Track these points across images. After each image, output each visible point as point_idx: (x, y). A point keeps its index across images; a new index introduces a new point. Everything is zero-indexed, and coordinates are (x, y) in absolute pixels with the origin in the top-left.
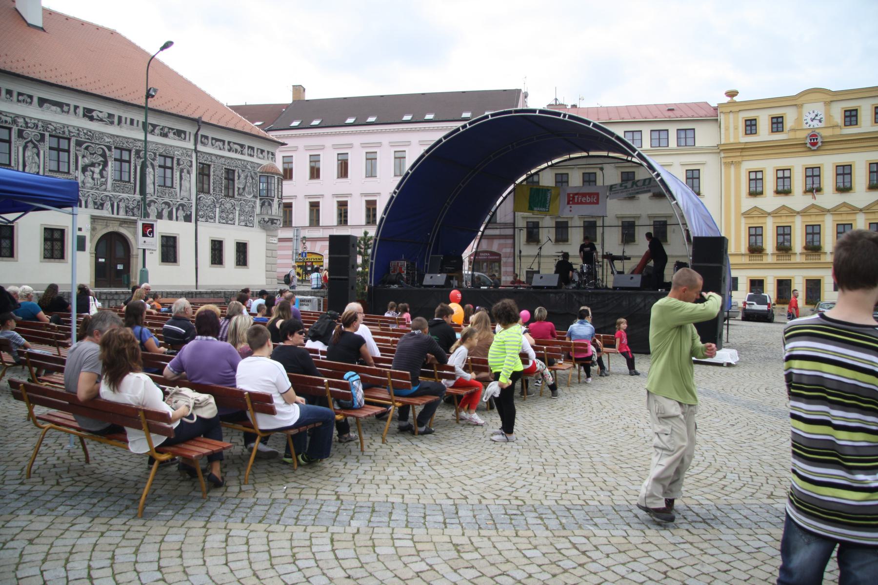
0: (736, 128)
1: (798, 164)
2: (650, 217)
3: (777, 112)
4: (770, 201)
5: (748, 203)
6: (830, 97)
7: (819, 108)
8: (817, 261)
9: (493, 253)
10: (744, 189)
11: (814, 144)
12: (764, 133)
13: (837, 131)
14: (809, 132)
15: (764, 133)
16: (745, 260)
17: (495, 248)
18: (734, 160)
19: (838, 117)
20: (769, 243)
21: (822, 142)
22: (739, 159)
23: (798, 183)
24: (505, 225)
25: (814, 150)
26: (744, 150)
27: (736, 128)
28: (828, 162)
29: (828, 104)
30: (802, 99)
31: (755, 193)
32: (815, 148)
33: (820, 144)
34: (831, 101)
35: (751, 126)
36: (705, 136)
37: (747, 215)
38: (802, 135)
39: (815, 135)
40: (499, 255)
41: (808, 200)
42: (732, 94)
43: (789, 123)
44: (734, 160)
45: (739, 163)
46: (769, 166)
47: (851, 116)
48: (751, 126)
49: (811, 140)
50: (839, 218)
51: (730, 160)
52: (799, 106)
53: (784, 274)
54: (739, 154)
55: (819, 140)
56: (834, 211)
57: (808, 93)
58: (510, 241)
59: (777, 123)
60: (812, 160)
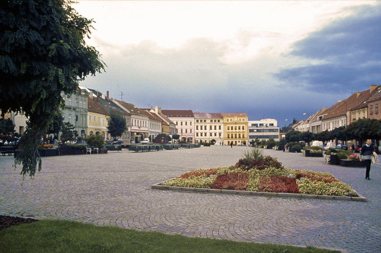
1: (234, 126)
4: (230, 131)
5: (228, 131)
10: (227, 129)
16: (227, 138)
17: (185, 137)
19: (239, 120)
20: (230, 137)
23: (234, 128)
24: (193, 133)
26: (227, 123)
28: (237, 126)
29: (237, 118)
35: (228, 120)
37: (227, 132)
41: (235, 131)
43: (233, 120)
45: (226, 125)
46: (230, 126)
52: (234, 118)
56: (238, 132)
60: (236, 125)
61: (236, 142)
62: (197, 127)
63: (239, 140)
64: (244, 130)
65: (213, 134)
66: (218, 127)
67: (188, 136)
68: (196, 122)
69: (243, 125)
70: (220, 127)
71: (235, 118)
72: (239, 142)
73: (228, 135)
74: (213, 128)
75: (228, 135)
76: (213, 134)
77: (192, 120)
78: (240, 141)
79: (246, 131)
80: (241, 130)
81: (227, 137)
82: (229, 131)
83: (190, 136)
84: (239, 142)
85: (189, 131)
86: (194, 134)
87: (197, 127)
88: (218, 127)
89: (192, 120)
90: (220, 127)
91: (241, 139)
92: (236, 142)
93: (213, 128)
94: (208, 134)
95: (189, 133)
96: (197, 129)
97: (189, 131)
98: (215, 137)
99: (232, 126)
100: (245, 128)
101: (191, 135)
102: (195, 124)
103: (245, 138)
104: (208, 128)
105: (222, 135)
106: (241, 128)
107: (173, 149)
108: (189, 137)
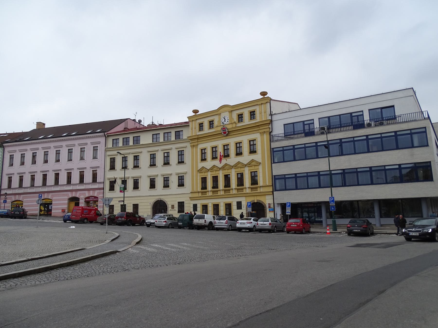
0: (195, 128)
1: (220, 143)
2: (162, 175)
3: (211, 119)
4: (209, 163)
6: (231, 109)
7: (226, 115)
8: (228, 194)
9: (96, 197)
11: (225, 133)
12: (206, 130)
13: (234, 125)
14: (222, 127)
15: (206, 130)
16: (200, 195)
18: (195, 144)
19: (235, 119)
21: (228, 131)
22: (196, 144)
24: (100, 183)
25: (225, 136)
27: (195, 128)
28: (232, 141)
30: (221, 110)
31: (204, 159)
32: (225, 135)
33: (227, 133)
34: (232, 111)
36: (186, 134)
37: (200, 171)
38: (219, 129)
39: (224, 128)
40: (98, 198)
42: (195, 111)
43: (216, 123)
44: (195, 144)
46: (208, 145)
47: (240, 117)
48: (201, 126)
49: (223, 131)
50: (237, 170)
51: (192, 144)
53: (216, 201)
54: (197, 141)
55: (227, 131)
57: (222, 108)
58: (102, 191)
59: (211, 123)
60: (225, 141)
61: (228, 206)
62: (113, 161)
63: (239, 199)
64: (257, 157)
65: (159, 183)
66: (174, 158)
67: (86, 192)
68: (110, 145)
69: (252, 137)
70: (181, 154)
71: (223, 115)
72: (239, 205)
73: (204, 180)
74: (160, 160)
75: (204, 180)
76: (159, 183)
77: (99, 143)
78: (244, 202)
79: (263, 157)
80: (246, 158)
81: (199, 189)
82: (204, 164)
83: (91, 193)
84: (239, 205)
85: (88, 178)
86: (101, 186)
87: (113, 161)
88: (174, 158)
89: (99, 143)
90: (181, 154)
91: (247, 195)
92: (228, 206)
93: (160, 160)
94: (144, 184)
95: (89, 184)
96: (113, 167)
97: (88, 178)
98: (167, 191)
99: (214, 144)
100: (259, 148)
101: (94, 189)
102: (109, 153)
103: (262, 190)
104: (145, 160)
105: (187, 181)
106: (246, 149)
107: (130, 226)
108: (87, 195)
